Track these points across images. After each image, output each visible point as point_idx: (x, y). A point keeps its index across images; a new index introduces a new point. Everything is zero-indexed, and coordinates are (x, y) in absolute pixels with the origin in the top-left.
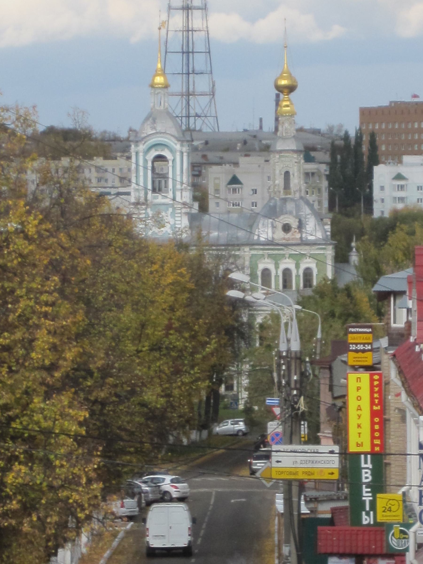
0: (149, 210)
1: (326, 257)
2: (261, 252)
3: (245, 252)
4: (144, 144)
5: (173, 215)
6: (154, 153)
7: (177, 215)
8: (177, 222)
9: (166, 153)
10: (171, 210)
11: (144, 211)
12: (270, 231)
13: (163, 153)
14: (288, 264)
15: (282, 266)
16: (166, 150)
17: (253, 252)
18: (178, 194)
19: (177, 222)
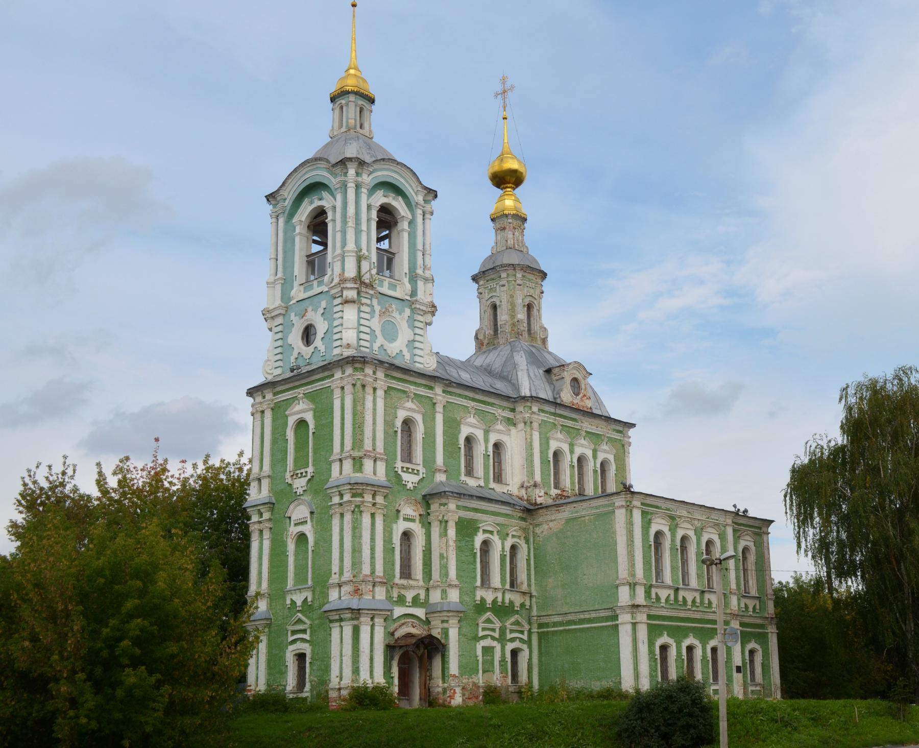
0: (375, 302)
1: (623, 446)
2: (551, 419)
3: (533, 413)
4: (371, 173)
5: (411, 321)
6: (380, 198)
7: (417, 324)
8: (418, 338)
9: (398, 204)
10: (408, 312)
11: (368, 302)
12: (548, 388)
13: (394, 203)
14: (583, 448)
15: (578, 451)
16: (400, 198)
17: (543, 417)
18: (420, 284)
19: (418, 338)
